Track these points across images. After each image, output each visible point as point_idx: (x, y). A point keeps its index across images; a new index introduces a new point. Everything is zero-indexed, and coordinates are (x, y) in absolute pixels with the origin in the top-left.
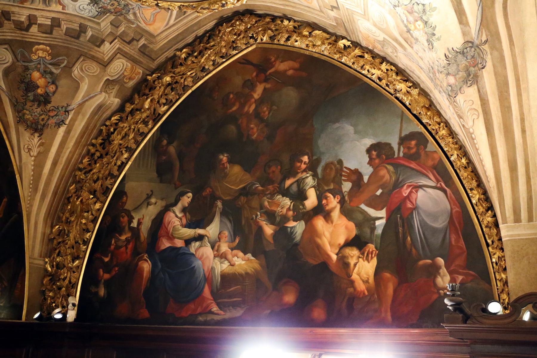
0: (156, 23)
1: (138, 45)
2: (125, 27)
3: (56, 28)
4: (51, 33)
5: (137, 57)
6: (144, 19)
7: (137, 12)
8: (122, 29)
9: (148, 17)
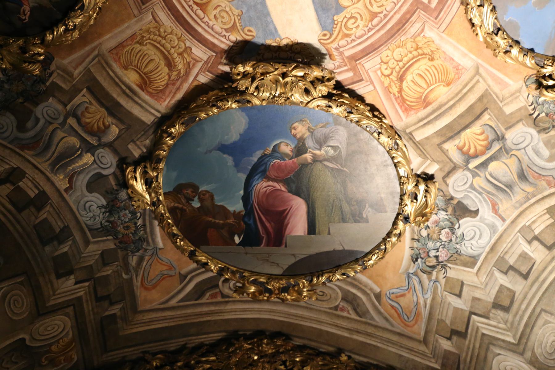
0: (154, 291)
1: (107, 310)
2: (113, 272)
3: (33, 210)
4: (20, 210)
5: (90, 331)
6: (146, 275)
7: (147, 258)
8: (108, 271)
9: (152, 275)
